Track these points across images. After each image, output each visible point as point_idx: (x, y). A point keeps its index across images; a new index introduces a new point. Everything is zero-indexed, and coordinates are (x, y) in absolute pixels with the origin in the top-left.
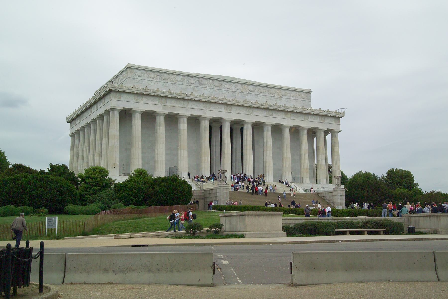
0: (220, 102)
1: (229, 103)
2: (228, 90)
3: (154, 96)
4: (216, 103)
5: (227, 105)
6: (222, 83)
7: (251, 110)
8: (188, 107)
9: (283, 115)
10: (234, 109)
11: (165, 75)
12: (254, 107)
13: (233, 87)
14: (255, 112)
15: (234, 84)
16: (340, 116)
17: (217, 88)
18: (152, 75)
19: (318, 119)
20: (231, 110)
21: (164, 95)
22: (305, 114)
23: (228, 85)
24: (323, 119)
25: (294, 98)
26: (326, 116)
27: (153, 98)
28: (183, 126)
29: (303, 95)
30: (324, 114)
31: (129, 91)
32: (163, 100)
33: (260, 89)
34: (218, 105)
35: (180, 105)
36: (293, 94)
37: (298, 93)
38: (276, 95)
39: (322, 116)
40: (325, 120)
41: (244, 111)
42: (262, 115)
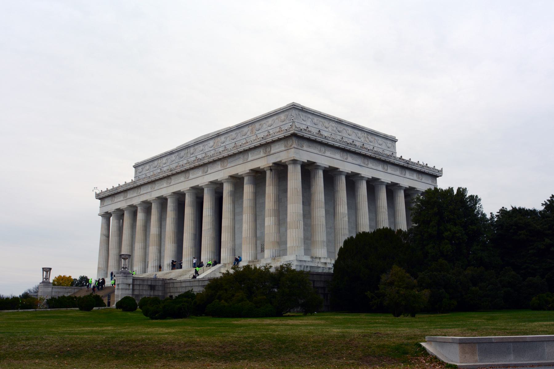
1: (165, 175)
6: (196, 147)
9: (218, 166)
10: (174, 180)
14: (192, 175)
18: (147, 167)
19: (261, 153)
20: (170, 183)
22: (240, 153)
25: (272, 127)
28: (140, 216)
30: (263, 142)
35: (135, 195)
36: (270, 121)
37: (275, 117)
39: (261, 146)
40: (270, 151)
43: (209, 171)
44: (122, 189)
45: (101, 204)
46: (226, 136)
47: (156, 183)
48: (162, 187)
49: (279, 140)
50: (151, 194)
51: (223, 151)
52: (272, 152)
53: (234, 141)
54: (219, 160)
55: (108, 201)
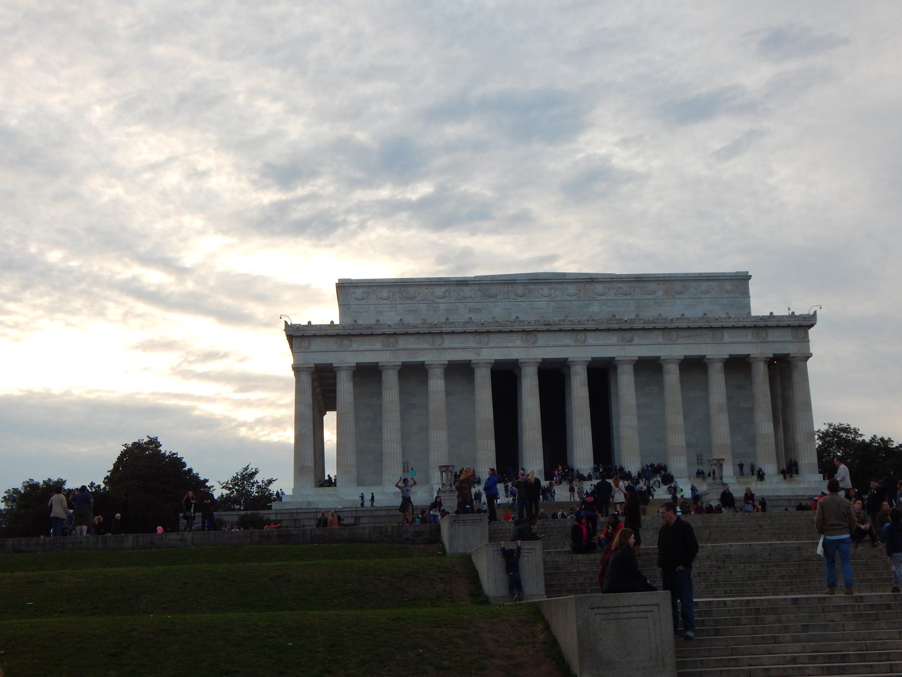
0: (509, 328)
1: (526, 328)
2: (547, 299)
3: (372, 335)
4: (500, 332)
5: (524, 331)
6: (531, 287)
7: (581, 336)
8: (444, 346)
9: (659, 337)
10: (542, 339)
11: (411, 290)
12: (585, 330)
13: (558, 293)
14: (591, 338)
15: (559, 286)
16: (803, 323)
17: (522, 299)
18: (385, 293)
19: (749, 336)
20: (535, 342)
21: (391, 331)
22: (711, 327)
23: (545, 290)
24: (762, 333)
26: (767, 327)
27: (371, 338)
28: (437, 384)
29: (728, 286)
31: (324, 333)
32: (392, 340)
33: (621, 288)
34: (505, 335)
35: (426, 346)
36: (704, 286)
37: (714, 283)
38: (660, 293)
39: (755, 327)
40: (767, 335)
41: (567, 339)
43: (636, 340)
46: (607, 285)
47: (492, 336)
48: (510, 345)
49: (789, 326)
51: (677, 319)
52: (770, 339)
53: (625, 297)
54: (665, 329)
55: (316, 345)
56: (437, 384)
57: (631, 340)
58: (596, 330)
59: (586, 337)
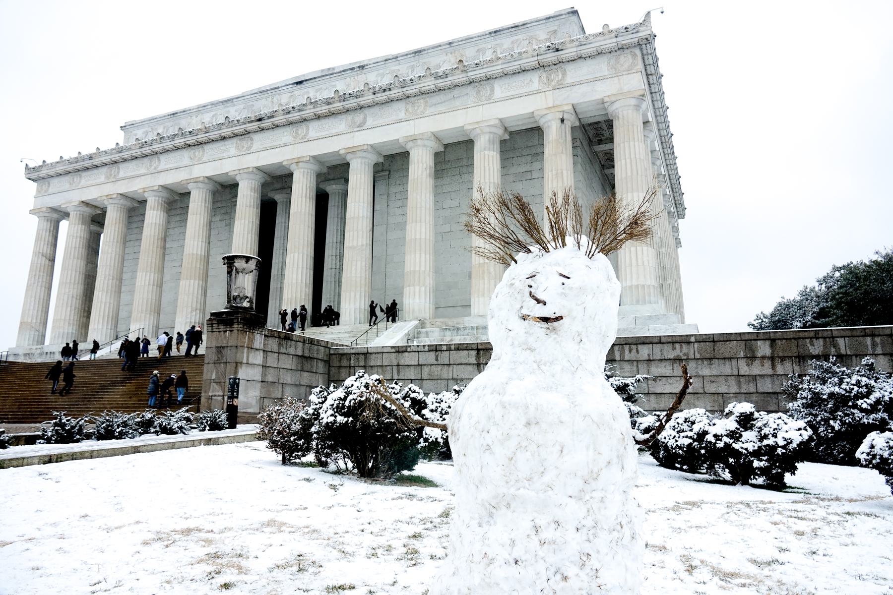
7: (302, 129)
8: (159, 169)
10: (259, 140)
14: (314, 129)
19: (534, 81)
20: (249, 148)
28: (154, 216)
32: (114, 169)
42: (334, 131)
43: (370, 122)
44: (106, 159)
45: (38, 191)
47: (207, 147)
48: (223, 155)
50: (195, 170)
52: (569, 80)
56: (154, 216)
57: (364, 122)
58: (318, 117)
59: (308, 129)
